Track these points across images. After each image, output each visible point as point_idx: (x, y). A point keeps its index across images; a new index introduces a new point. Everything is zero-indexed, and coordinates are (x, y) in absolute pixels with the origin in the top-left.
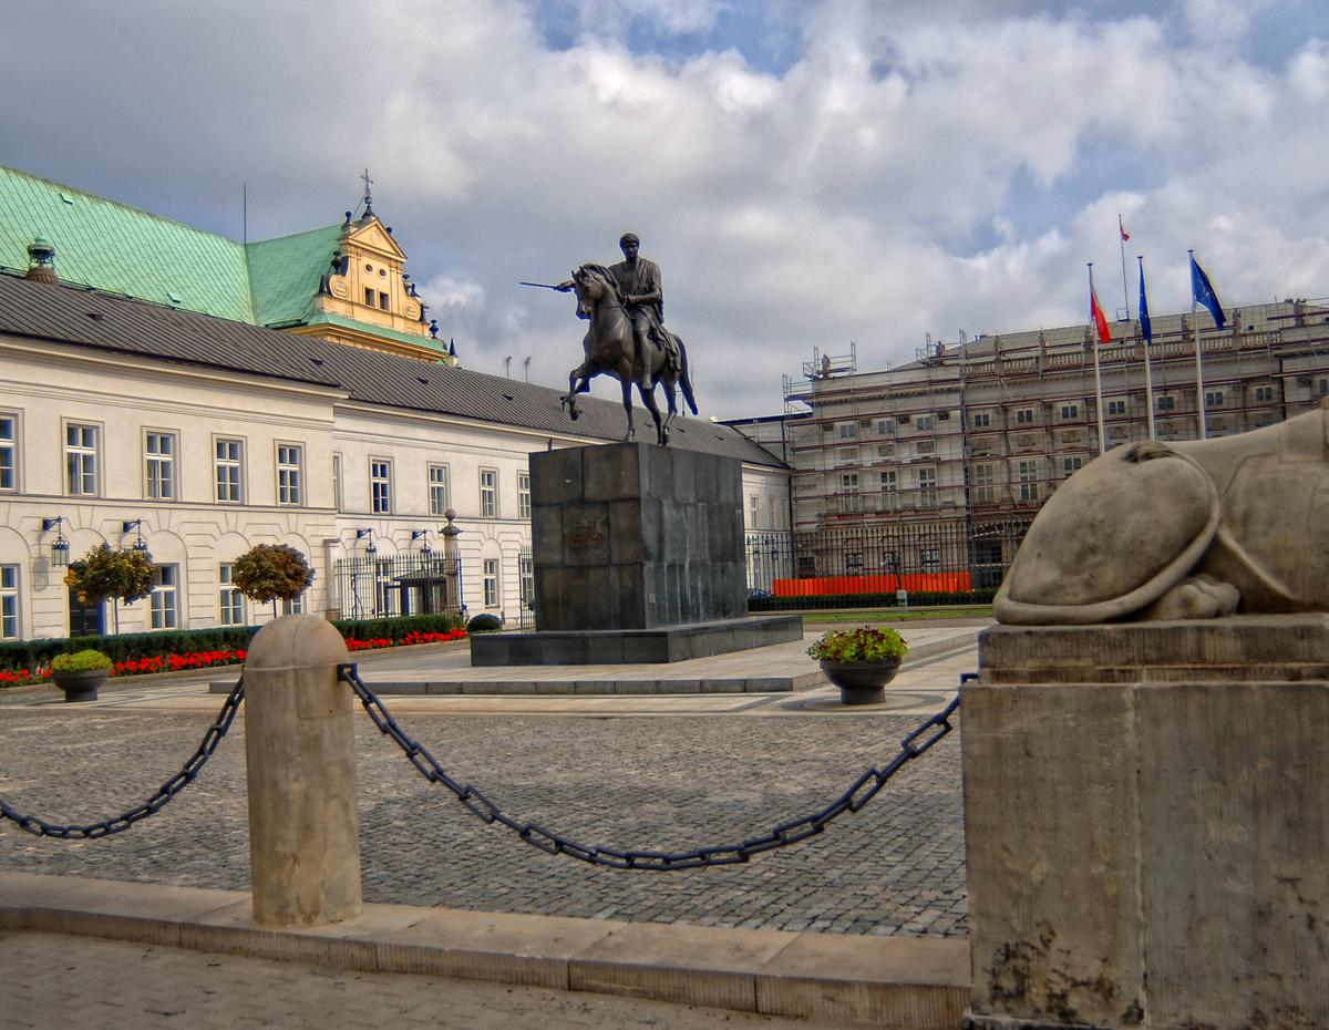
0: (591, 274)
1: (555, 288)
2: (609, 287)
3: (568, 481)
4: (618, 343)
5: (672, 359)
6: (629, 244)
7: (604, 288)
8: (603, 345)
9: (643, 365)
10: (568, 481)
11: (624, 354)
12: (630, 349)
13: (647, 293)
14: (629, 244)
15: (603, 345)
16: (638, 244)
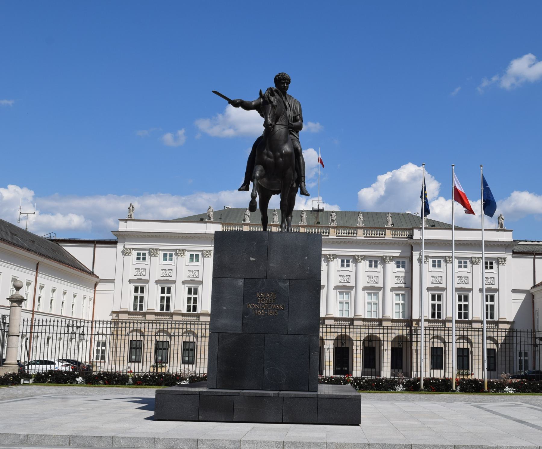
4: (288, 155)
13: (294, 122)
16: (289, 83)
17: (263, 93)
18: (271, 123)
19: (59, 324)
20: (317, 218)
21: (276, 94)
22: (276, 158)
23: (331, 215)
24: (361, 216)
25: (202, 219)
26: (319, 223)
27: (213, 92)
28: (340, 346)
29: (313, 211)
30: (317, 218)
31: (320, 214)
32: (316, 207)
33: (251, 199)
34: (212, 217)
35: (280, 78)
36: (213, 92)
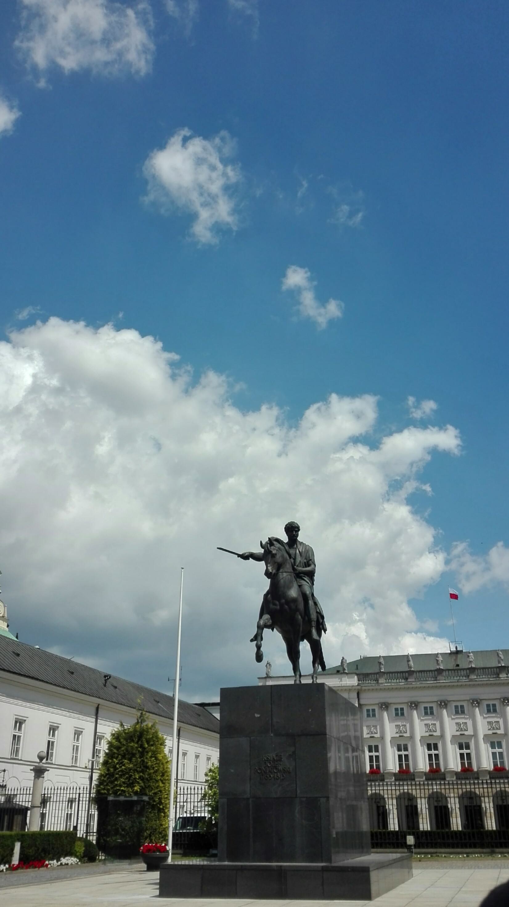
0: (277, 545)
1: (239, 556)
2: (288, 558)
3: (257, 715)
4: (294, 600)
5: (321, 621)
6: (292, 529)
7: (283, 556)
8: (283, 601)
9: (310, 621)
10: (257, 715)
11: (297, 610)
12: (301, 606)
13: (306, 567)
14: (292, 529)
15: (283, 601)
16: (299, 530)
17: (264, 543)
18: (271, 571)
19: (193, 792)
20: (456, 660)
21: (275, 543)
22: (281, 605)
23: (468, 656)
24: (440, 656)
25: (338, 671)
26: (458, 665)
27: (218, 548)
28: (500, 803)
29: (452, 653)
30: (456, 660)
31: (459, 656)
32: (453, 649)
33: (256, 649)
34: (346, 669)
35: (292, 527)
36: (218, 548)
